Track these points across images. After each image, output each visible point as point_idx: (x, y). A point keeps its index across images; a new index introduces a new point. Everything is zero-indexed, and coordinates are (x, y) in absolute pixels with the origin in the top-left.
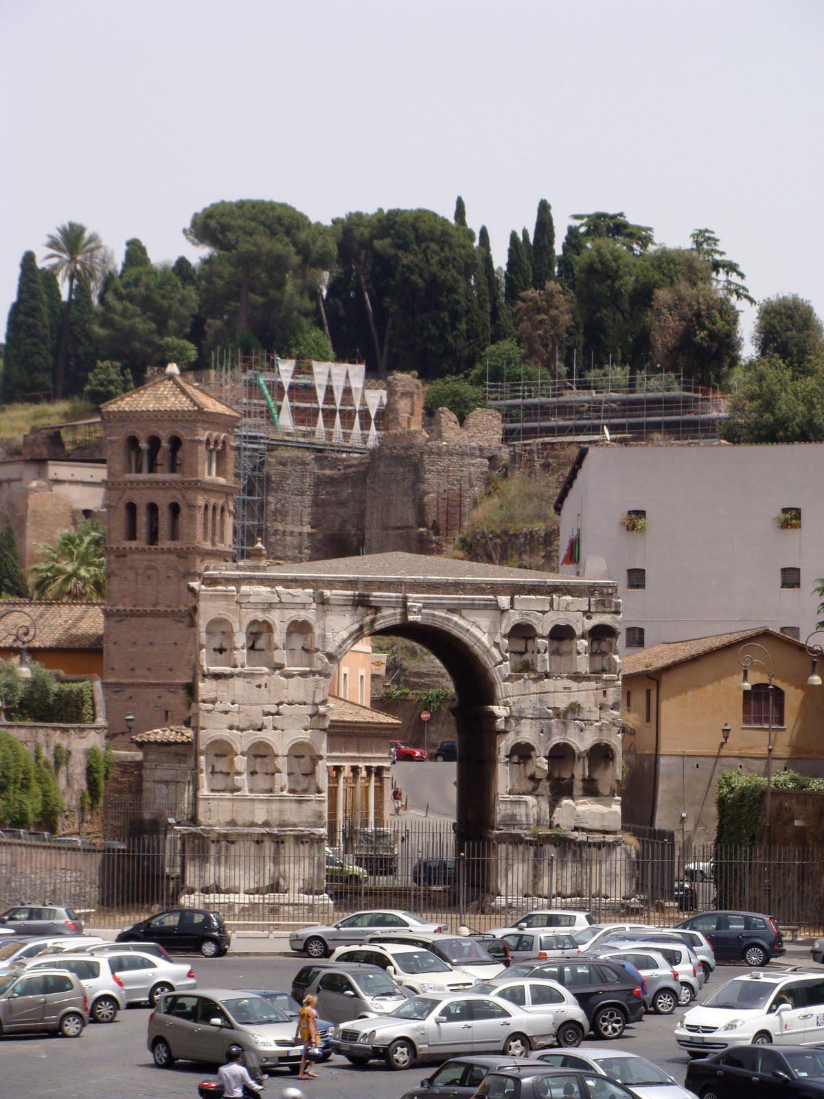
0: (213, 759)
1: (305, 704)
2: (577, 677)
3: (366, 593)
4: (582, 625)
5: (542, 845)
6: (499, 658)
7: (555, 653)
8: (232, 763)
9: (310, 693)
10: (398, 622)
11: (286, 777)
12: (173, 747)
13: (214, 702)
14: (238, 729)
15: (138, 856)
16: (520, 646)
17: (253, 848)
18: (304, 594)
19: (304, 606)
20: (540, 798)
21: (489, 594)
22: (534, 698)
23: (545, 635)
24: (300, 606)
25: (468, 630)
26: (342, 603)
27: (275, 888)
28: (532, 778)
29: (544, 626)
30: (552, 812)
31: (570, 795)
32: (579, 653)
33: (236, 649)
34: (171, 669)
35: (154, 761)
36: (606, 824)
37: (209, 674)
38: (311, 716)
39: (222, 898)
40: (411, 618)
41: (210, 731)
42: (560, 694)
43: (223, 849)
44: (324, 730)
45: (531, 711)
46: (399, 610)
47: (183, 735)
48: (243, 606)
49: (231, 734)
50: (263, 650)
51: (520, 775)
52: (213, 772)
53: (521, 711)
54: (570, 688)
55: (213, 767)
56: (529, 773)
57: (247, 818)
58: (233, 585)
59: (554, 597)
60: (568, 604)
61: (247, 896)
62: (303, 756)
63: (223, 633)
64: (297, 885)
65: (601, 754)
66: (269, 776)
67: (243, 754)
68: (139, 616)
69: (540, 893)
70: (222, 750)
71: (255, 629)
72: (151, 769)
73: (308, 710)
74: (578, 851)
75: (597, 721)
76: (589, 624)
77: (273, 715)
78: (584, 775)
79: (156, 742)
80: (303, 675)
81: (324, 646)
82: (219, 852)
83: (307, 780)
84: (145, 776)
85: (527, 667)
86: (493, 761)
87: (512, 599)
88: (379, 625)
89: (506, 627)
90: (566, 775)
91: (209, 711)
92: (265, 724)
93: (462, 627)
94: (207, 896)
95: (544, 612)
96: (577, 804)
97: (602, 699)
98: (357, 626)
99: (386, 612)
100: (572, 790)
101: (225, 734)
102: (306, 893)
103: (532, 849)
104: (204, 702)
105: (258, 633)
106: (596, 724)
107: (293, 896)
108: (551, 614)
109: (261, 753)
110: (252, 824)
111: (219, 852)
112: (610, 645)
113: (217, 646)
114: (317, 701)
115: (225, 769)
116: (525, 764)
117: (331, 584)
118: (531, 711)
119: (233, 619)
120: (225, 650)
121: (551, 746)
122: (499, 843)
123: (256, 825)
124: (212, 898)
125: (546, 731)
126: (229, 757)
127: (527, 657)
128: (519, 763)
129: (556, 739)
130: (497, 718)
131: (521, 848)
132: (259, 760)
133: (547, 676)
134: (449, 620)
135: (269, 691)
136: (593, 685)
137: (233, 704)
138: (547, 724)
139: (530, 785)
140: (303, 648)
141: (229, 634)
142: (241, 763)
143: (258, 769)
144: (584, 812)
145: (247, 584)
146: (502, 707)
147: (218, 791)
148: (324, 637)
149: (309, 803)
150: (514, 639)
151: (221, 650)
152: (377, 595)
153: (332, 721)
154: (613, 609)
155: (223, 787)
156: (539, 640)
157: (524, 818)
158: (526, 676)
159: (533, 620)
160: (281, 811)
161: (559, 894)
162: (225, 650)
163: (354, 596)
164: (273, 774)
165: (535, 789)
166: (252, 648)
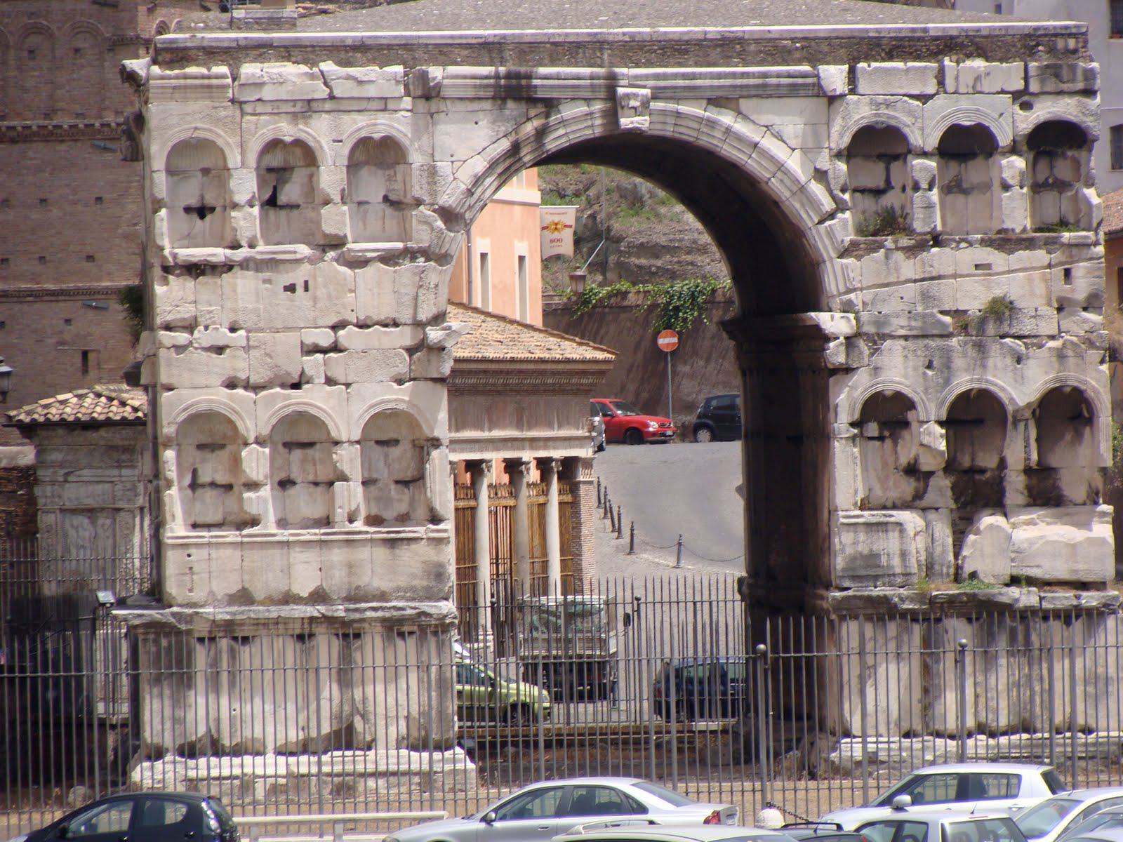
0: (192, 455)
1: (396, 324)
2: (1005, 241)
3: (523, 69)
4: (1011, 123)
5: (938, 620)
6: (828, 205)
7: (954, 188)
8: (236, 461)
9: (408, 300)
10: (598, 131)
11: (360, 489)
12: (103, 432)
13: (190, 327)
14: (247, 386)
15: (34, 680)
16: (873, 175)
17: (291, 648)
18: (384, 78)
19: (385, 104)
20: (932, 515)
21: (799, 62)
22: (910, 291)
23: (928, 148)
25: (756, 145)
26: (470, 94)
27: (344, 738)
28: (912, 470)
29: (925, 130)
30: (958, 545)
31: (997, 503)
32: (1006, 187)
33: (235, 206)
34: (90, 258)
35: (61, 465)
36: (1081, 566)
37: (177, 265)
38: (411, 351)
39: (226, 766)
40: (626, 122)
41: (184, 392)
42: (968, 279)
43: (225, 657)
44: (441, 380)
45: (904, 322)
46: (598, 106)
47: (123, 404)
48: (248, 108)
49: (231, 398)
50: (297, 206)
51: (885, 464)
52: (194, 486)
53: (881, 321)
54: (988, 266)
55: (195, 473)
56: (904, 461)
57: (277, 584)
58: (223, 62)
59: (947, 61)
60: (978, 79)
61: (282, 759)
62: (396, 442)
63: (206, 171)
64: (393, 730)
65: (1064, 411)
67: (260, 442)
68: (13, 141)
69: (939, 726)
71: (276, 160)
72: (53, 483)
73: (405, 336)
74: (1020, 628)
75: (1053, 337)
76: (1027, 121)
77: (324, 351)
78: (1027, 459)
79: (63, 423)
80: (389, 259)
81: (433, 194)
83: (406, 494)
84: (41, 501)
85: (892, 223)
86: (823, 436)
87: (852, 72)
88: (553, 143)
89: (841, 134)
90: (988, 461)
91: (179, 349)
92: (309, 372)
93: (740, 138)
94: (191, 763)
95: (924, 98)
96: (1014, 526)
97: (1062, 288)
98: (505, 144)
99: (570, 111)
100: (1001, 493)
101: (219, 398)
102: (414, 748)
103: (917, 630)
104: (168, 327)
105: (284, 166)
106: (1052, 344)
107: (385, 757)
110: (288, 599)
112: (1077, 164)
113: (194, 201)
114: (423, 316)
115: (221, 478)
116: (895, 439)
117: (443, 52)
118: (904, 322)
119: (227, 140)
120: (212, 210)
121: (952, 398)
122: (843, 618)
123: (297, 600)
124: (203, 767)
125: (939, 365)
126: (230, 448)
127: (892, 199)
128: (881, 438)
129: (963, 382)
130: (827, 338)
131: (892, 628)
132: (297, 454)
133: (937, 240)
134: (712, 124)
136: (1041, 256)
137: (233, 330)
138: (941, 349)
139: (907, 487)
140: (386, 199)
141: (218, 173)
142: (256, 462)
143: (296, 474)
144: (1031, 542)
146: (838, 315)
147: (209, 526)
148: (432, 172)
149: (414, 547)
150: (857, 161)
151: (202, 211)
152: (546, 73)
153: (457, 361)
154: (1080, 85)
155: (218, 518)
156: (917, 162)
157: (896, 562)
158: (889, 242)
159: (900, 117)
160: (351, 567)
161: (981, 729)
162: (212, 210)
163: (497, 76)
164: (331, 484)
165: (919, 496)
166: (271, 202)
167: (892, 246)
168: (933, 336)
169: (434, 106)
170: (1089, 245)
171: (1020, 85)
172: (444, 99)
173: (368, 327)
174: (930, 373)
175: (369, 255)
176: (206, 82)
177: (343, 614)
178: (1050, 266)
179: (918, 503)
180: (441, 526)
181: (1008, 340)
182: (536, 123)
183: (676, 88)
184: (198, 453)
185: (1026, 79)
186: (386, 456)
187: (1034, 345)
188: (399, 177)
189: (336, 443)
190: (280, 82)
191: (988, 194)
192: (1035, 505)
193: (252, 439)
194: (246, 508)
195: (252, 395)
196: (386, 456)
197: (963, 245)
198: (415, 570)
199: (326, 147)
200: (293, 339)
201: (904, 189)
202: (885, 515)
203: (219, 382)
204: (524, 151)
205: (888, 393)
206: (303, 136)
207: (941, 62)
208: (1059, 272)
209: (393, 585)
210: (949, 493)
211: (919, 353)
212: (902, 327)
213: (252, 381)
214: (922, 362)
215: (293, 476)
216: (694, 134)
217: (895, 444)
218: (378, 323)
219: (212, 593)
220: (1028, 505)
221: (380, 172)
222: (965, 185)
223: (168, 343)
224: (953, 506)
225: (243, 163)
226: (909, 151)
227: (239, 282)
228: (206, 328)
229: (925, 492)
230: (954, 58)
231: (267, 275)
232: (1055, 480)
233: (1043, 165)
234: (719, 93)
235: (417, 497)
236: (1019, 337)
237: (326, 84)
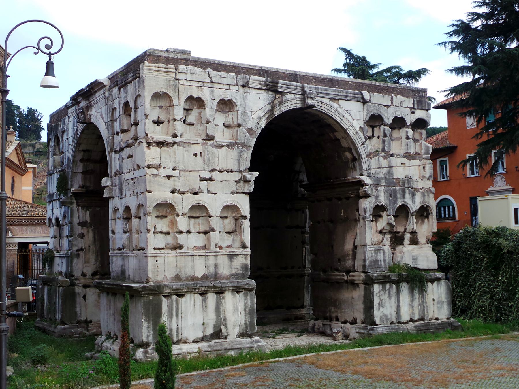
1: (232, 171)
2: (408, 156)
4: (410, 119)
8: (173, 223)
10: (299, 106)
17: (198, 298)
24: (226, 87)
26: (259, 87)
29: (388, 117)
32: (408, 138)
38: (237, 182)
43: (174, 303)
48: (181, 82)
54: (404, 164)
56: (379, 228)
60: (401, 102)
62: (226, 217)
65: (423, 212)
66: (202, 235)
67: (183, 215)
70: (166, 209)
77: (206, 180)
90: (401, 229)
95: (388, 107)
97: (423, 173)
98: (269, 107)
100: (403, 239)
104: (149, 167)
106: (421, 191)
108: (391, 109)
109: (199, 211)
113: (156, 119)
115: (165, 230)
116: (376, 221)
120: (162, 123)
121: (397, 207)
128: (372, 221)
129: (399, 203)
131: (388, 286)
132: (193, 220)
135: (204, 161)
137: (174, 170)
139: (381, 236)
140: (224, 125)
142: (183, 223)
145: (186, 64)
147: (159, 249)
155: (162, 246)
157: (383, 263)
160: (216, 266)
161: (412, 320)
169: (246, 89)
173: (221, 172)
174: (391, 198)
175: (224, 144)
176: (166, 70)
178: (420, 165)
182: (279, 100)
184: (156, 220)
185: (413, 104)
186: (223, 222)
188: (230, 116)
189: (210, 217)
191: (400, 141)
193: (180, 214)
194: (179, 242)
195: (180, 195)
196: (223, 222)
197: (398, 156)
198: (238, 267)
199: (209, 101)
200: (196, 175)
201: (379, 137)
204: (275, 110)
208: (422, 167)
209: (230, 273)
213: (181, 191)
214: (389, 195)
216: (326, 110)
217: (376, 223)
219: (165, 276)
221: (222, 114)
223: (150, 173)
225: (179, 104)
226: (382, 125)
227: (177, 151)
228: (164, 168)
231: (187, 149)
235: (235, 238)
237: (209, 76)
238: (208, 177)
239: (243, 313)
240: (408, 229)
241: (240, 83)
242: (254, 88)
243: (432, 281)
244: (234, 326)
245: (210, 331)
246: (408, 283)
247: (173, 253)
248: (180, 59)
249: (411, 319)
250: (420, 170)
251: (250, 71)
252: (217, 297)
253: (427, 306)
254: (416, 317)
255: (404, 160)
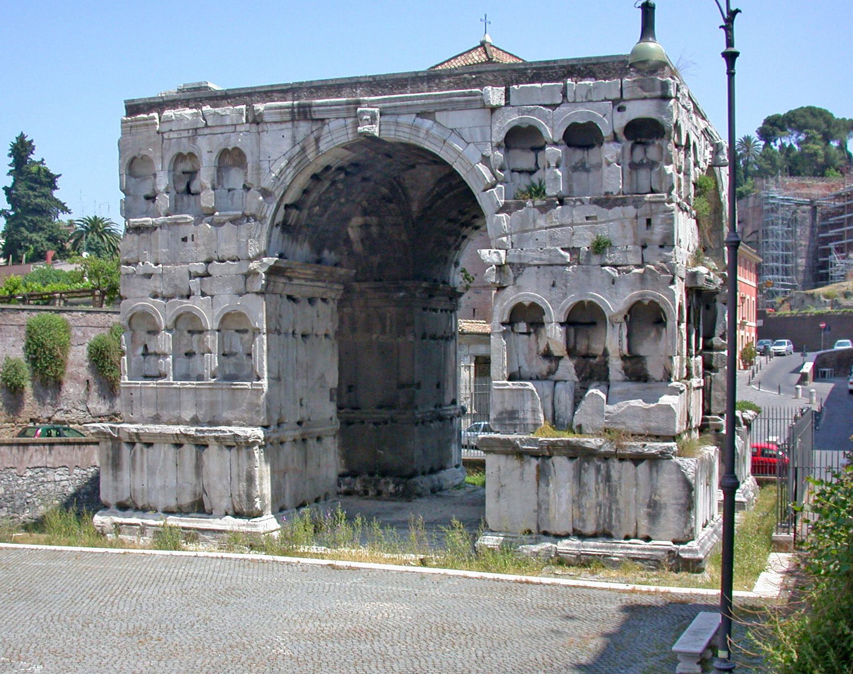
2: (606, 202)
4: (611, 122)
14: (163, 298)
16: (525, 160)
17: (172, 451)
24: (231, 129)
26: (278, 119)
28: (547, 355)
32: (609, 164)
36: (652, 424)
48: (166, 136)
51: (530, 349)
54: (595, 218)
55: (146, 347)
56: (542, 348)
62: (245, 331)
67: (168, 330)
71: (186, 166)
75: (638, 266)
76: (621, 121)
78: (621, 350)
81: (259, 180)
82: (133, 460)
85: (538, 191)
87: (507, 91)
95: (554, 106)
98: (298, 148)
99: (334, 124)
101: (149, 303)
111: (133, 460)
112: (661, 149)
113: (149, 192)
116: (536, 332)
128: (528, 334)
132: (196, 337)
136: (630, 210)
139: (543, 366)
140: (244, 186)
142: (165, 342)
143: (195, 349)
148: (258, 169)
154: (659, 93)
163: (293, 107)
165: (551, 372)
167: (531, 205)
168: (557, 265)
170: (663, 202)
171: (616, 95)
172: (266, 123)
173: (223, 261)
177: (193, 433)
178: (637, 217)
179: (551, 377)
180: (260, 382)
181: (607, 268)
183: (396, 107)
184: (147, 336)
186: (242, 338)
187: (624, 271)
190: (180, 119)
192: (631, 381)
196: (242, 338)
202: (522, 385)
203: (147, 294)
204: (309, 151)
205: (527, 303)
206: (191, 150)
207: (565, 83)
210: (573, 371)
211: (547, 276)
212: (536, 259)
215: (194, 350)
216: (408, 136)
217: (537, 339)
218: (229, 259)
220: (625, 381)
222: (587, 166)
224: (577, 379)
227: (160, 237)
229: (557, 369)
230: (574, 79)
232: (643, 365)
233: (639, 151)
234: (423, 109)
236: (615, 266)
237: (204, 119)
238: (201, 271)
239: (235, 480)
240: (610, 350)
241: (250, 120)
242: (276, 122)
243: (637, 459)
244: (221, 497)
245: (187, 499)
246: (571, 458)
247: (152, 383)
248: (168, 101)
249: (574, 530)
250: (635, 228)
251: (267, 93)
252: (197, 452)
253: (618, 509)
254: (590, 529)
255: (594, 210)
